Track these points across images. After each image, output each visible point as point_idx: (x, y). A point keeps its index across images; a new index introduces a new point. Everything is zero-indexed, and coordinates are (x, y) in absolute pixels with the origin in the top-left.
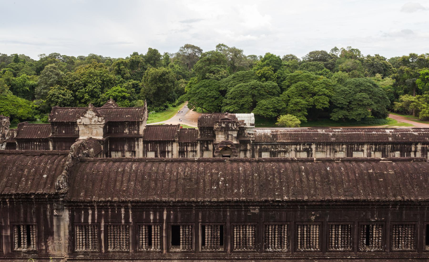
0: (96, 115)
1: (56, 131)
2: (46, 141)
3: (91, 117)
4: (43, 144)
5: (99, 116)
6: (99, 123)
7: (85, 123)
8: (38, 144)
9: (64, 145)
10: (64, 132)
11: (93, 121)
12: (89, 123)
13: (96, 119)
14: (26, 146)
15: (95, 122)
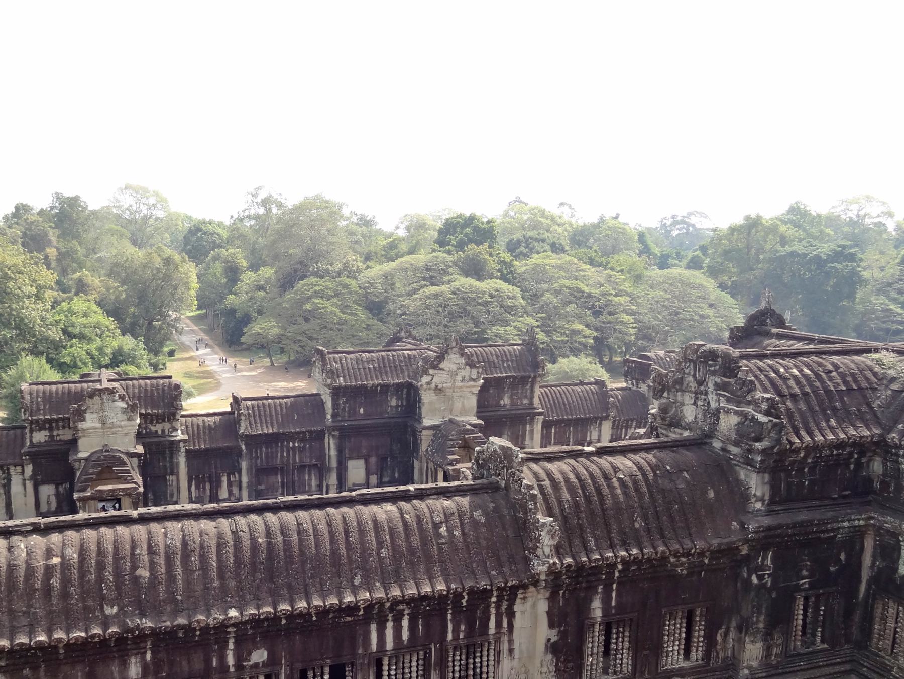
0: (467, 364)
1: (344, 409)
2: (319, 436)
3: (454, 367)
4: (311, 446)
5: (471, 365)
6: (472, 383)
7: (440, 386)
8: (299, 446)
9: (364, 443)
10: (362, 411)
11: (459, 378)
12: (450, 385)
13: (466, 372)
14: (267, 454)
15: (463, 381)
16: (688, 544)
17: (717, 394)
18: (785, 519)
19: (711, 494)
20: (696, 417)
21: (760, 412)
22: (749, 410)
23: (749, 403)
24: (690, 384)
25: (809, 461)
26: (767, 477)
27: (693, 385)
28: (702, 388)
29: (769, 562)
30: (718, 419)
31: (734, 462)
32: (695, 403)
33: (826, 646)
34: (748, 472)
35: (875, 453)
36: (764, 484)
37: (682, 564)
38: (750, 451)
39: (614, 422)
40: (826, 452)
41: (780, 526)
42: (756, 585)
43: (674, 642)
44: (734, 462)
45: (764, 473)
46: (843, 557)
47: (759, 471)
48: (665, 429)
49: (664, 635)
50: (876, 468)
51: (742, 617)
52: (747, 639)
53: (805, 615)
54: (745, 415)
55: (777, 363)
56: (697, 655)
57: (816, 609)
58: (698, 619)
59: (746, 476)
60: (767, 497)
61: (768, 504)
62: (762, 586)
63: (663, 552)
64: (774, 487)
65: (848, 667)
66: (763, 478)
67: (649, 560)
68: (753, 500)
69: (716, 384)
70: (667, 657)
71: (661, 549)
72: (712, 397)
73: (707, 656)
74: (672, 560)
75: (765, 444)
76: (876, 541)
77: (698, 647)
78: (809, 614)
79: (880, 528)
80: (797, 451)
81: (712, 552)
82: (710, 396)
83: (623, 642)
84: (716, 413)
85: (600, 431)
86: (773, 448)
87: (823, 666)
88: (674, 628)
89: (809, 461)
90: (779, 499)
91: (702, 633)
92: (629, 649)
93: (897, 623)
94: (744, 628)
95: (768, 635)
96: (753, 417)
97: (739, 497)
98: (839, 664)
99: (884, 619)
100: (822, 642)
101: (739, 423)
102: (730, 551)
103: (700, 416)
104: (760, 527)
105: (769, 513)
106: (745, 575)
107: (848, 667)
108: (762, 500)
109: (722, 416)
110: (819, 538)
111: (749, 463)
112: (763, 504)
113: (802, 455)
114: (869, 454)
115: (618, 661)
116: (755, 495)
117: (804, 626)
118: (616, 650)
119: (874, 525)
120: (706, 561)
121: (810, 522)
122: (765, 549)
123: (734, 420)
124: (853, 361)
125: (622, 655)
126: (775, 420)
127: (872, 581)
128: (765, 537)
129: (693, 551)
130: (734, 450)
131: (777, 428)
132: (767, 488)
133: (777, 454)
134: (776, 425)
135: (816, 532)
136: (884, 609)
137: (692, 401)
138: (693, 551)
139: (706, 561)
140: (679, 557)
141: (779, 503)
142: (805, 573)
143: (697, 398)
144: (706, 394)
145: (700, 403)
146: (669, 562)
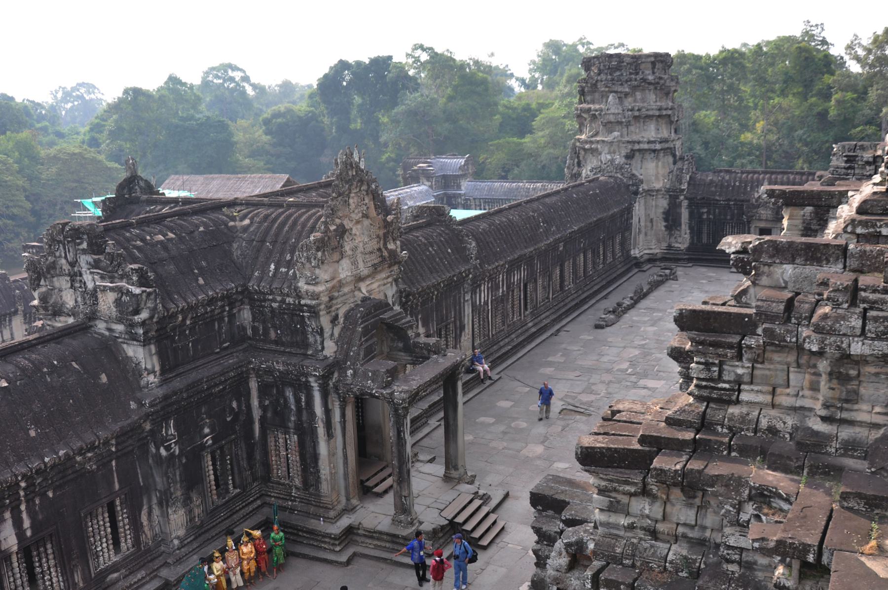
16: (90, 438)
17: (91, 273)
18: (178, 384)
19: (104, 378)
20: (76, 301)
21: (133, 285)
22: (123, 284)
23: (121, 278)
24: (64, 267)
25: (188, 322)
26: (153, 348)
27: (66, 267)
28: (76, 269)
29: (172, 431)
30: (97, 299)
31: (120, 340)
32: (72, 287)
33: (238, 490)
34: (135, 348)
35: (243, 303)
36: (151, 355)
37: (90, 459)
38: (132, 325)
39: (25, 316)
40: (201, 310)
41: (175, 393)
42: (166, 457)
43: (100, 540)
44: (120, 340)
45: (150, 344)
46: (234, 405)
47: (145, 343)
48: (50, 320)
49: (89, 537)
50: (246, 316)
51: (160, 491)
52: (170, 511)
53: (215, 470)
54: (119, 290)
55: (143, 230)
56: (126, 545)
57: (223, 460)
58: (119, 508)
59: (135, 352)
60: (157, 368)
61: (161, 375)
62: (172, 456)
63: (66, 454)
64: (162, 355)
65: (259, 502)
66: (150, 350)
67: (53, 467)
68: (145, 374)
69: (88, 263)
70: (98, 557)
71: (61, 453)
72: (87, 277)
73: (137, 542)
74: (78, 459)
75: (144, 315)
76: (258, 382)
77: (126, 535)
78: (218, 467)
79: (259, 370)
80: (174, 316)
81: (117, 437)
82: (85, 276)
83: (47, 562)
84: (94, 294)
85: (11, 329)
86: (151, 318)
87: (241, 509)
88: (99, 525)
89: (188, 322)
90: (168, 369)
91: (126, 521)
92: (56, 566)
93: (287, 450)
94: (165, 502)
95: (187, 501)
96: (128, 290)
97: (129, 375)
98: (252, 502)
99: (277, 449)
100: (235, 487)
101: (116, 300)
102: (135, 429)
103: (79, 299)
104: (154, 400)
105: (164, 382)
106: (154, 450)
107: (259, 502)
108: (154, 372)
109: (100, 295)
110: (212, 394)
111: (134, 337)
112: (155, 376)
113: (180, 318)
114: (237, 304)
115: (47, 583)
116: (146, 369)
117: (216, 480)
118: (42, 572)
119: (253, 369)
120: (113, 449)
121: (200, 381)
122: (166, 419)
123: (111, 297)
124: (210, 219)
125: (50, 574)
126: (148, 290)
127: (263, 420)
128: (163, 408)
129: (97, 443)
130: (120, 328)
131: (152, 297)
132: (155, 359)
133: (156, 322)
134: (149, 294)
135: (208, 389)
136: (276, 441)
137: (69, 285)
138: (97, 443)
139: (113, 449)
140: (85, 453)
141: (171, 370)
142: (207, 430)
143: (72, 281)
144: (81, 275)
145: (77, 285)
146: (76, 462)
